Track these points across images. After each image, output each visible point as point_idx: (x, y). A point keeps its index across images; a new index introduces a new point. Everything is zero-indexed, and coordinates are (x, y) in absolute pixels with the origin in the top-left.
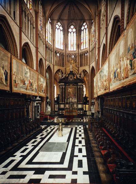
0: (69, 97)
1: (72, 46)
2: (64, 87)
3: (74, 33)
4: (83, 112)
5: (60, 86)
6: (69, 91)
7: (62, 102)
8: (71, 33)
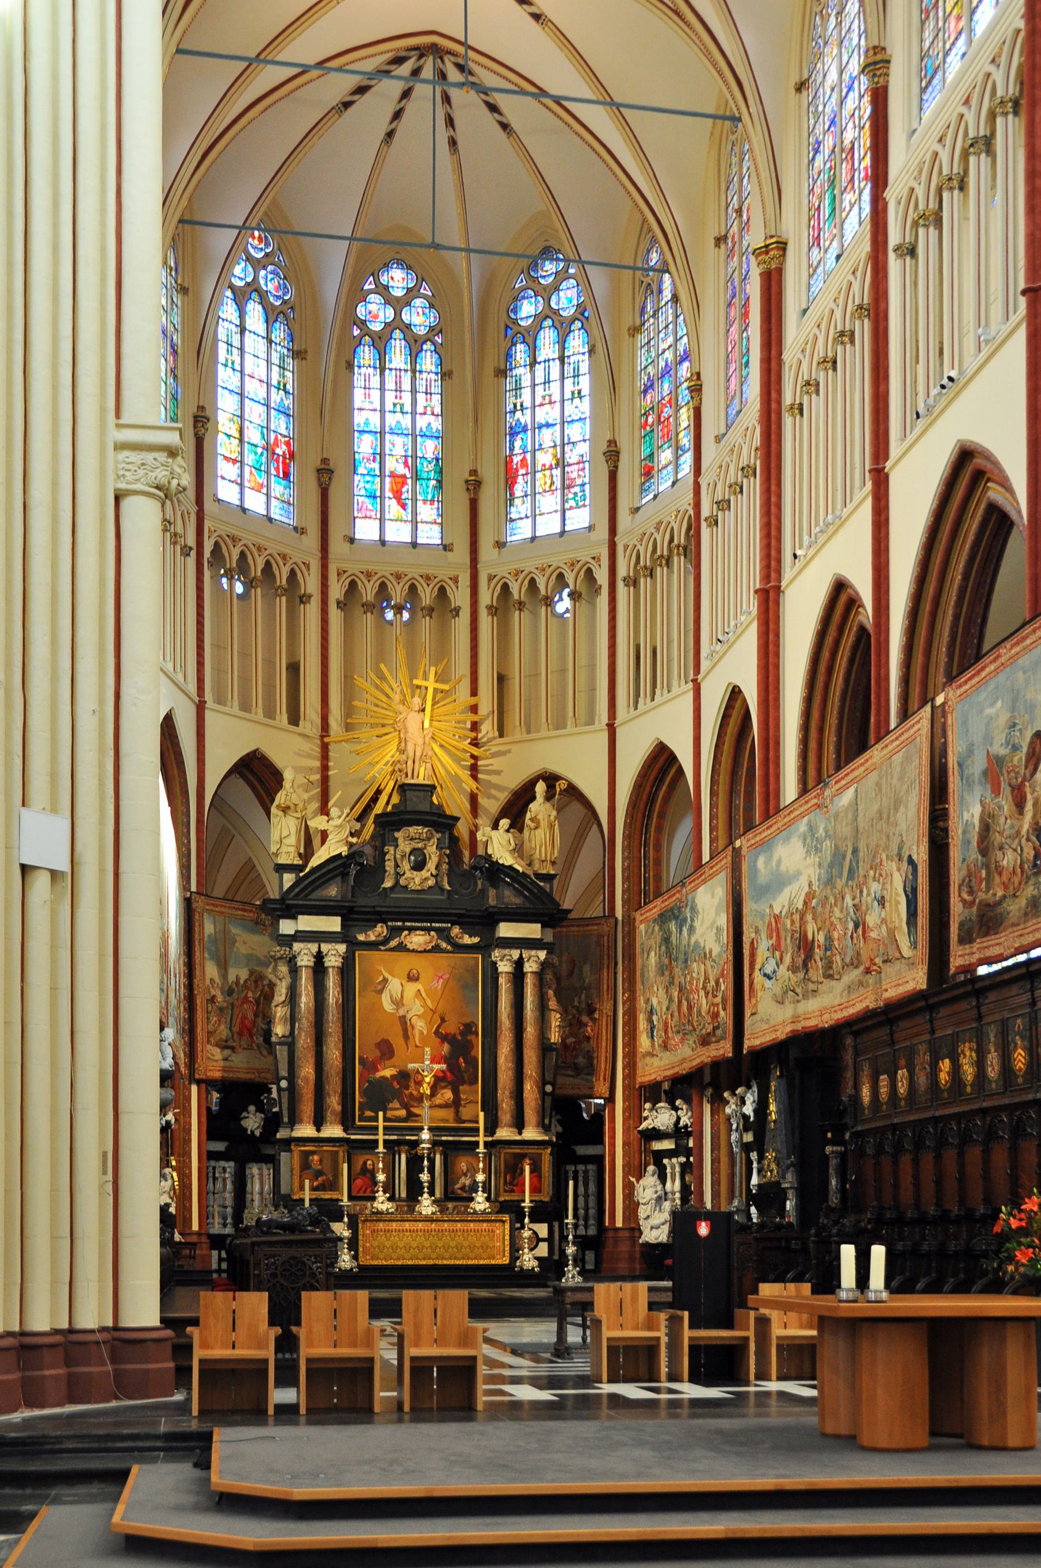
0: (388, 1073)
1: (397, 495)
2: (334, 954)
3: (415, 345)
4: (549, 1240)
5: (297, 946)
6: (398, 1003)
7: (319, 1122)
8: (380, 342)
